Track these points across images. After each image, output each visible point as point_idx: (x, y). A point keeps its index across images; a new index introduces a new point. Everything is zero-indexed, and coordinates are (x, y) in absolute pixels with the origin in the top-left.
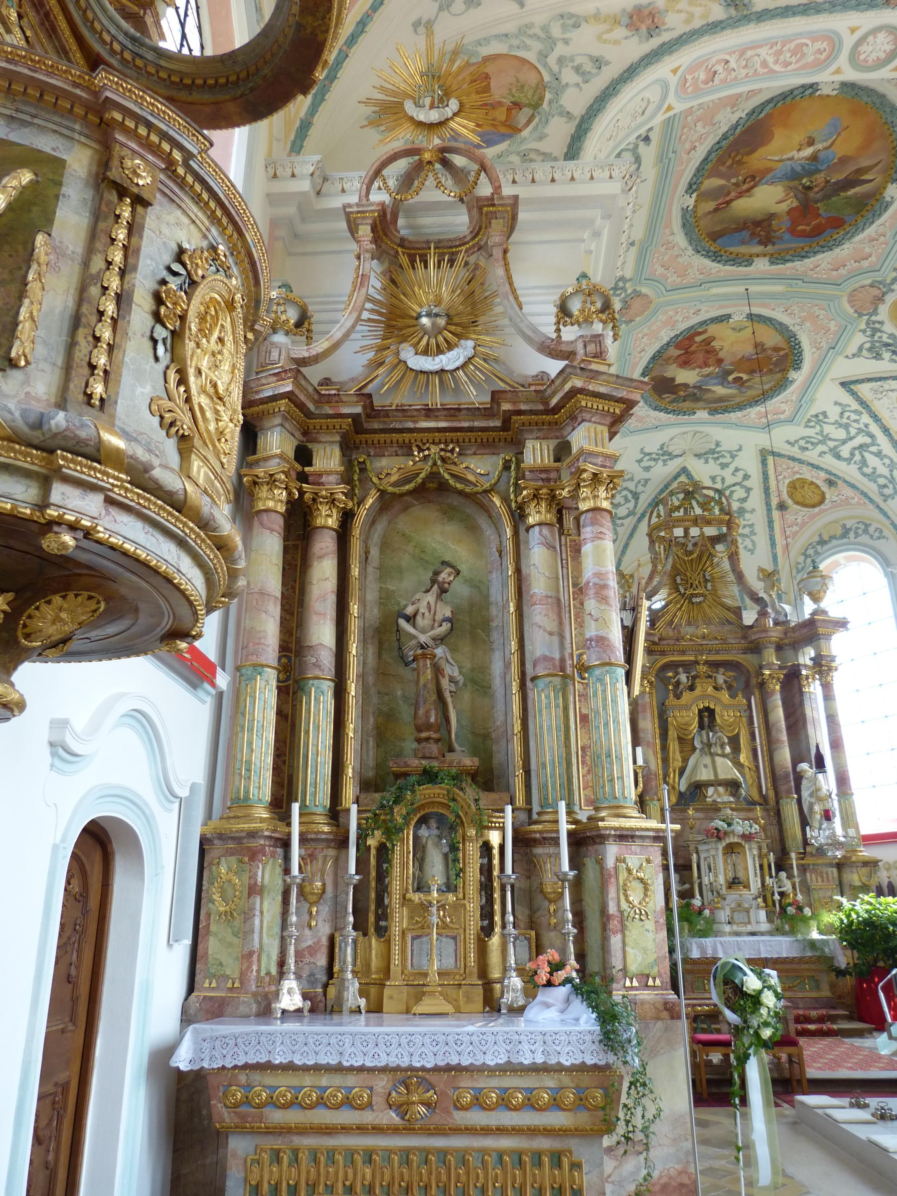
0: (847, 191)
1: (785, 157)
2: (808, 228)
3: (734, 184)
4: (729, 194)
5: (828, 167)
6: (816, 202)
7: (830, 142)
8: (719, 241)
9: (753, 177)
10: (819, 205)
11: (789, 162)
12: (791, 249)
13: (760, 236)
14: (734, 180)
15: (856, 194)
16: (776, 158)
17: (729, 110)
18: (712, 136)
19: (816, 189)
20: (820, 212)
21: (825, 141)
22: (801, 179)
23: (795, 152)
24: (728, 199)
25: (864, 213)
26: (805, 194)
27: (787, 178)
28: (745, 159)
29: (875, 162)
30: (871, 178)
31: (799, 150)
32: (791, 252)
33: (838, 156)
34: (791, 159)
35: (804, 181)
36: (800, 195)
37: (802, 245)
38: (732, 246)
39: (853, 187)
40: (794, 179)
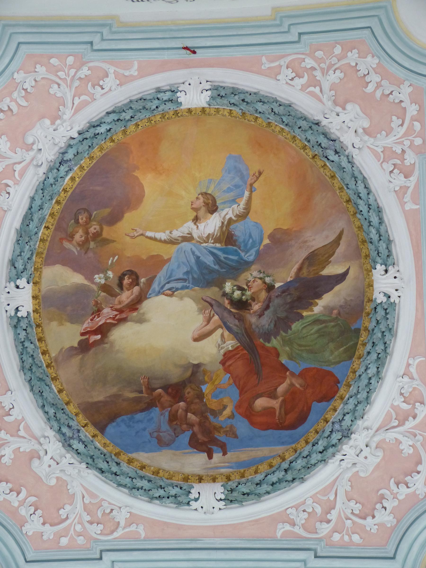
0: (309, 306)
1: (176, 234)
2: (275, 404)
3: (105, 288)
4: (98, 312)
5: (258, 254)
6: (267, 336)
7: (243, 203)
8: (111, 429)
9: (136, 282)
10: (275, 343)
11: (186, 246)
12: (261, 461)
13: (191, 425)
14: (99, 279)
15: (329, 309)
16: (163, 236)
17: (47, 122)
18: (31, 171)
19: (256, 307)
20: (284, 360)
21: (234, 201)
22: (220, 285)
23: (190, 224)
24: (100, 321)
25: (361, 350)
26: (241, 319)
27: (196, 282)
28: (107, 232)
29: (332, 238)
30: (340, 270)
31: (196, 220)
32: (263, 468)
33: (268, 230)
34: (188, 238)
35: (228, 287)
36: (233, 322)
37: (279, 449)
38: (138, 448)
39: (319, 296)
40: (208, 284)
